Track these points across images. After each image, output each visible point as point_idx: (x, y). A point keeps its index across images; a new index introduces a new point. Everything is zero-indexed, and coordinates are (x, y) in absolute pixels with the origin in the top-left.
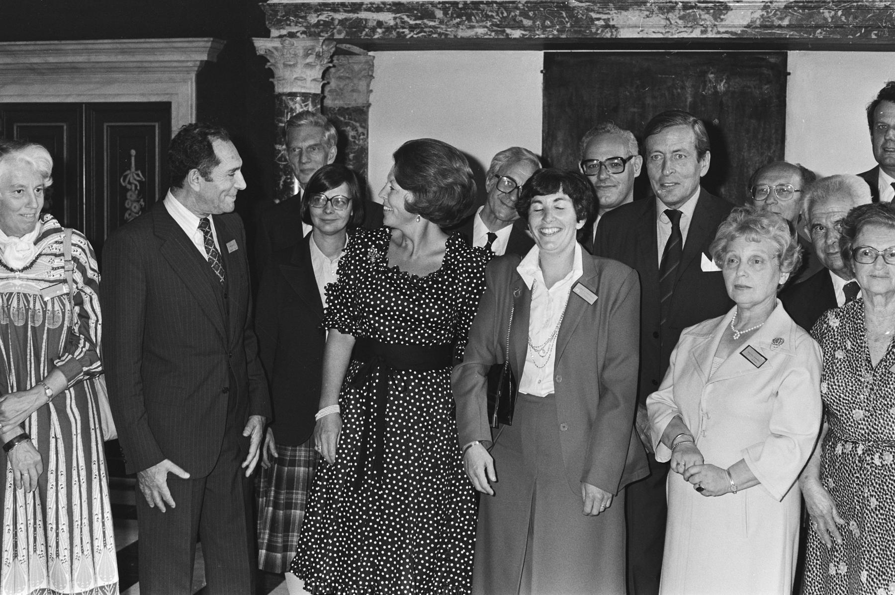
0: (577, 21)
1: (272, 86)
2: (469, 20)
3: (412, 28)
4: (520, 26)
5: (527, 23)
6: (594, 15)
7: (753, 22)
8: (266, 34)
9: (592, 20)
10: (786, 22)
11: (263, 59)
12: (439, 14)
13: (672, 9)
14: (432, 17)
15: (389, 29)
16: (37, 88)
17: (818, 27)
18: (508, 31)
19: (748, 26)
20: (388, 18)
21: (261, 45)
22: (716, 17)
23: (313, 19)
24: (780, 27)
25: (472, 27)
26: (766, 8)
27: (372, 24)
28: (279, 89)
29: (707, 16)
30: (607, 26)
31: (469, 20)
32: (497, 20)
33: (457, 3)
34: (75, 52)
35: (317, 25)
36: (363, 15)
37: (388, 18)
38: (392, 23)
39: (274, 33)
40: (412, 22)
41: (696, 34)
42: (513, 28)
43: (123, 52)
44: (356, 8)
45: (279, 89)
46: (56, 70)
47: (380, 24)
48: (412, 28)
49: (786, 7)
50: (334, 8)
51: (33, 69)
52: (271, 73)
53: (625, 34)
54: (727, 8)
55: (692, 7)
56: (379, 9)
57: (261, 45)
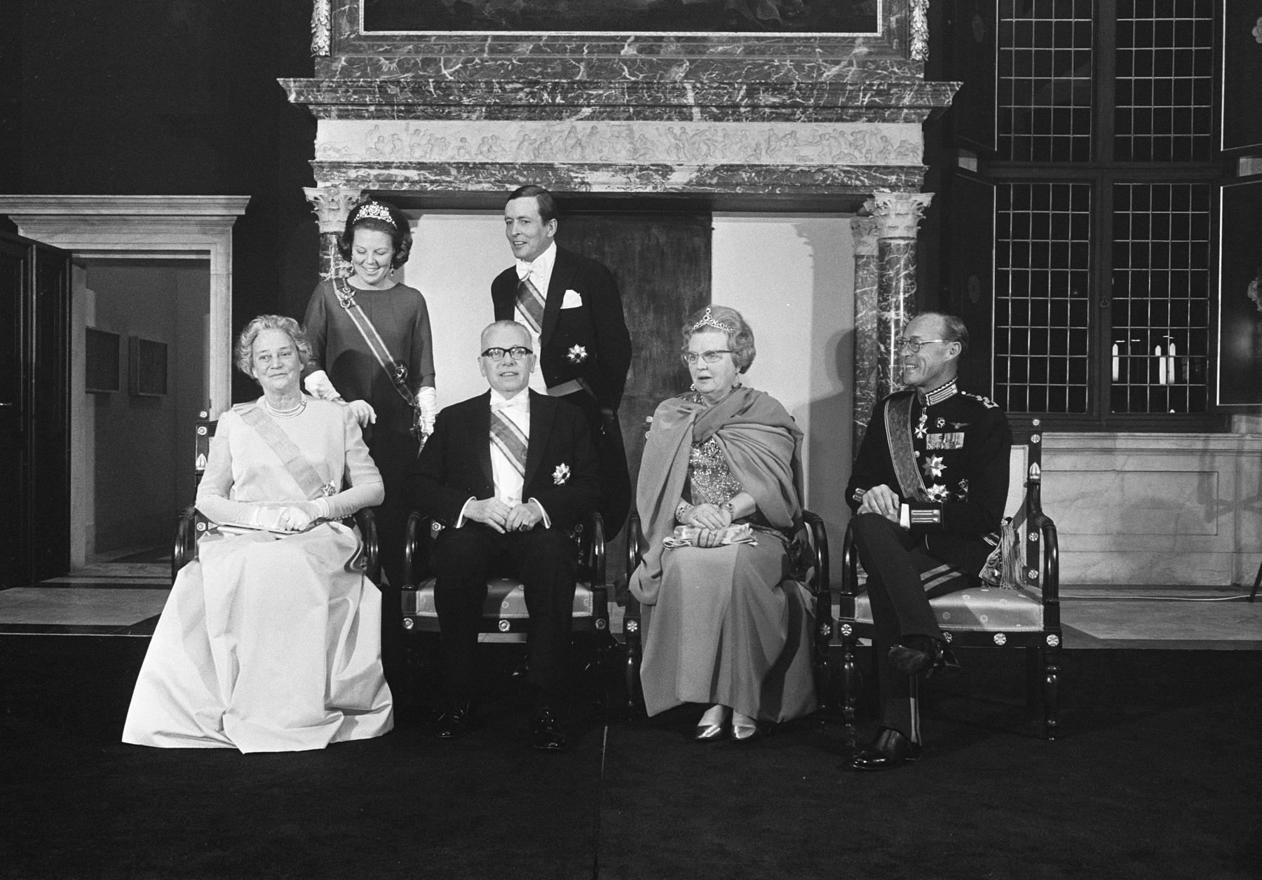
0: (560, 181)
1: (317, 227)
2: (477, 176)
3: (432, 182)
4: (517, 182)
5: (521, 179)
6: (573, 174)
7: (691, 181)
8: (314, 185)
9: (572, 178)
10: (715, 181)
11: (311, 205)
12: (454, 172)
13: (631, 170)
14: (448, 174)
15: (414, 183)
16: (87, 237)
17: (738, 185)
18: (507, 186)
19: (687, 184)
20: (413, 174)
21: (310, 193)
22: (664, 176)
23: (353, 174)
24: (710, 185)
25: (480, 182)
26: (700, 170)
27: (399, 179)
28: (323, 229)
29: (656, 176)
30: (583, 183)
31: (477, 176)
32: (499, 177)
33: (467, 164)
34: (126, 205)
35: (355, 180)
36: (393, 171)
37: (413, 174)
38: (417, 178)
39: (320, 184)
40: (433, 178)
41: (649, 189)
42: (511, 183)
43: (170, 206)
44: (387, 166)
45: (323, 229)
46: (106, 220)
47: (407, 179)
48: (432, 182)
49: (715, 170)
50: (370, 166)
51: (84, 219)
52: (317, 218)
53: (595, 189)
54: (672, 171)
55: (647, 169)
56: (406, 168)
57: (310, 193)
